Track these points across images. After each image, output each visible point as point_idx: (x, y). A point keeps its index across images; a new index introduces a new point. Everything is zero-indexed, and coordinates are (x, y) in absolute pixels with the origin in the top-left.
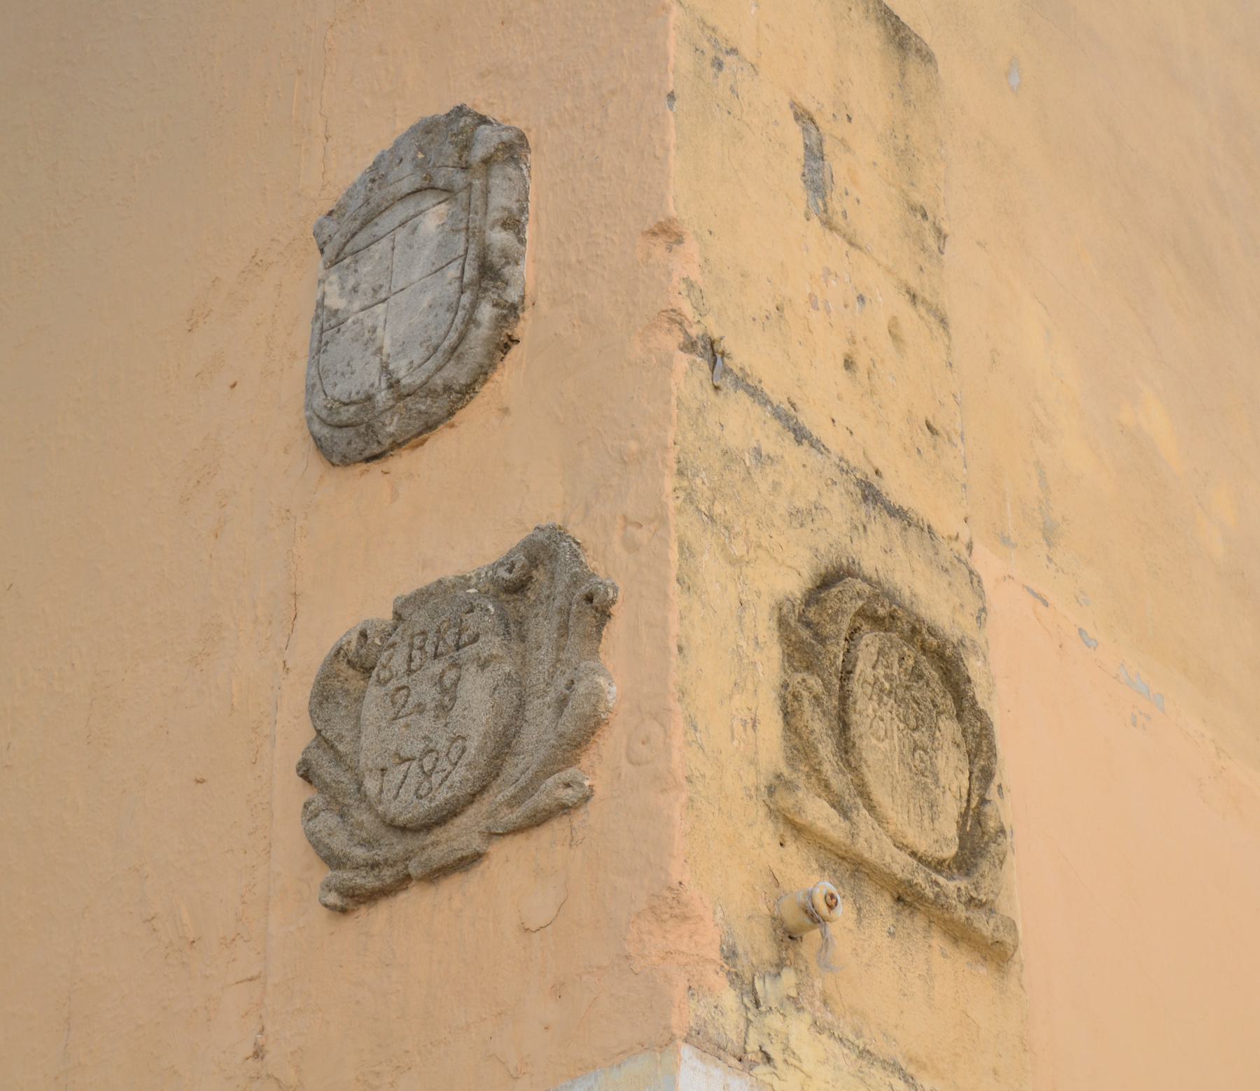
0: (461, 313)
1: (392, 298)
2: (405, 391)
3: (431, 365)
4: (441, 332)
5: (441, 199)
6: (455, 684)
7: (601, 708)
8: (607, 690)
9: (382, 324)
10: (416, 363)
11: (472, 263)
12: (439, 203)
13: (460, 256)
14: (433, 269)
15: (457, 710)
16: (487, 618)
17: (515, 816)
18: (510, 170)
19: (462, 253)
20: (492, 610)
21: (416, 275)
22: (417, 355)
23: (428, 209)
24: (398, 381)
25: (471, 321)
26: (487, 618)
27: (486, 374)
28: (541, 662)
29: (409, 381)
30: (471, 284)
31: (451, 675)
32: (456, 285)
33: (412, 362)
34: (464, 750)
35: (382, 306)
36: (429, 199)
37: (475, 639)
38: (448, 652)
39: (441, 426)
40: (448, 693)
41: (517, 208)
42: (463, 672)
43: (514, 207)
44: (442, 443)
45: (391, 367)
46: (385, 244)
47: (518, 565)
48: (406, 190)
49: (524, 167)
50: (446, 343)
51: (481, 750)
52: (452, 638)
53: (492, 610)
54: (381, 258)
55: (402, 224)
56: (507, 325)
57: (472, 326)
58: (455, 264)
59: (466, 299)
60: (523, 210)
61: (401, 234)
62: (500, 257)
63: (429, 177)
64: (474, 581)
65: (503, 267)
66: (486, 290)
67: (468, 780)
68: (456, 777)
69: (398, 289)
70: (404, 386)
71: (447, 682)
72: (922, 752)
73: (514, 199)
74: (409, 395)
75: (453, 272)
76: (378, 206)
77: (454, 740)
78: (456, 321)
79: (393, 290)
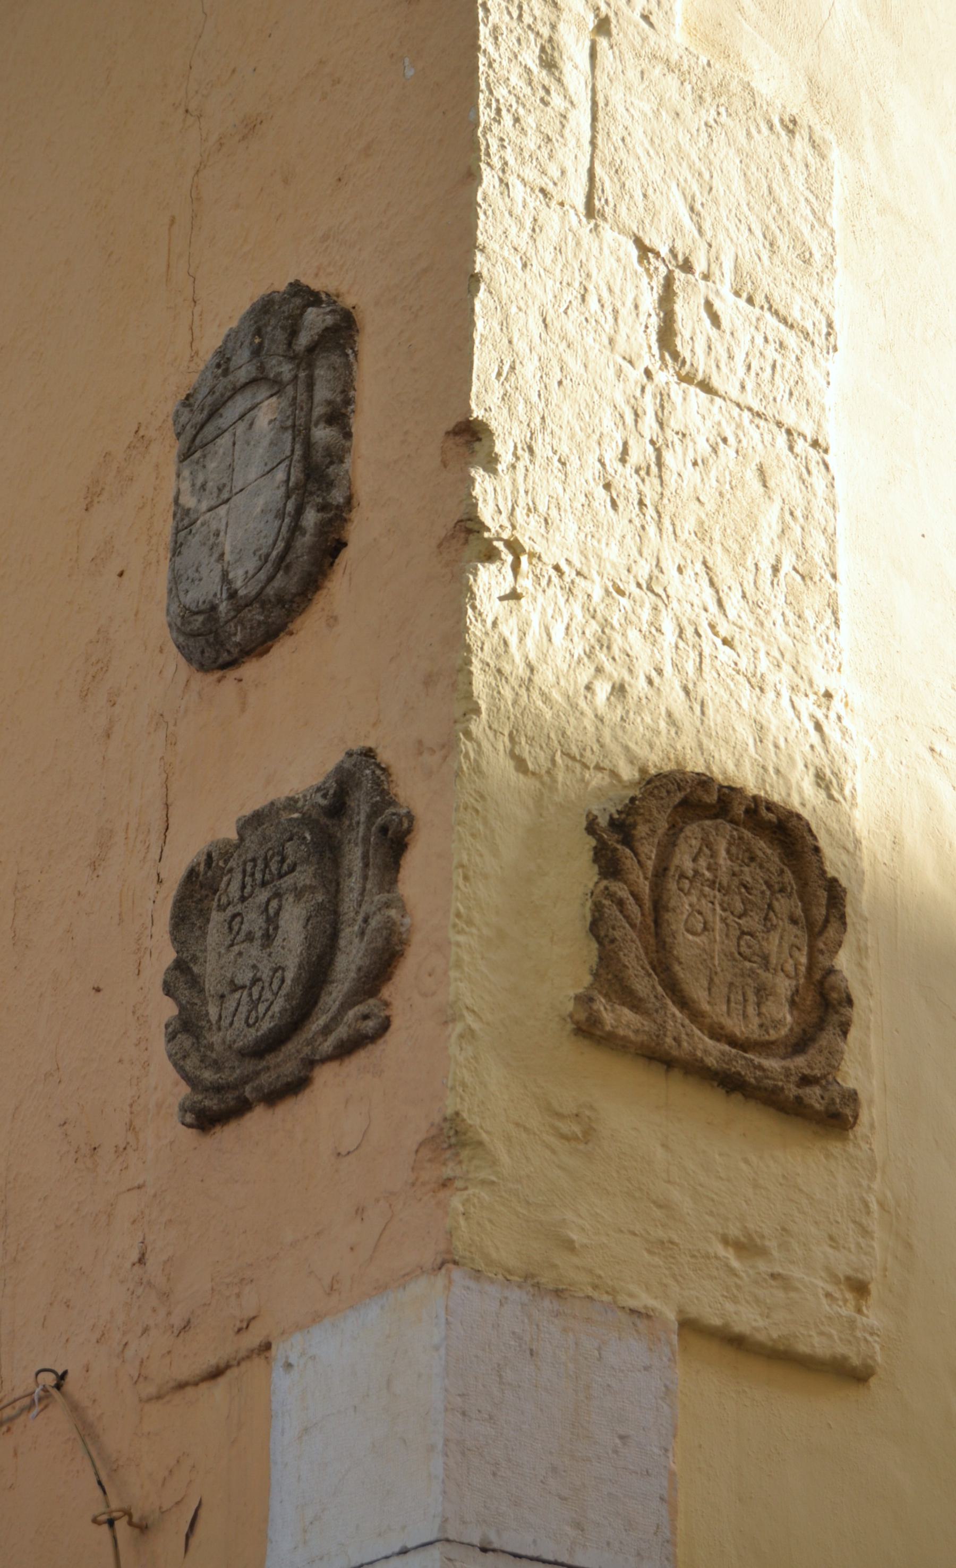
0: (287, 520)
1: (234, 498)
2: (242, 602)
3: (262, 576)
4: (270, 541)
5: (274, 391)
6: (277, 913)
7: (395, 939)
8: (399, 923)
9: (223, 528)
10: (251, 573)
11: (298, 465)
12: (272, 396)
13: (287, 457)
14: (267, 469)
15: (278, 941)
16: (303, 847)
17: (328, 1045)
18: (336, 359)
19: (288, 453)
20: (308, 837)
21: (253, 473)
22: (251, 564)
23: (262, 402)
24: (236, 592)
25: (296, 528)
26: (303, 847)
27: (316, 581)
28: (351, 890)
29: (245, 592)
30: (297, 487)
31: (274, 904)
32: (283, 489)
33: (247, 572)
34: (283, 981)
35: (224, 508)
36: (263, 392)
37: (292, 869)
38: (272, 881)
39: (282, 634)
40: (272, 921)
41: (342, 400)
42: (284, 902)
43: (338, 399)
44: (282, 651)
45: (231, 576)
46: (225, 440)
47: (331, 792)
48: (243, 380)
49: (350, 352)
50: (274, 553)
51: (296, 980)
52: (276, 866)
53: (308, 837)
54: (224, 454)
55: (241, 417)
56: (332, 529)
57: (297, 533)
58: (283, 466)
59: (290, 507)
60: (348, 402)
61: (241, 427)
62: (324, 457)
63: (261, 368)
64: (300, 804)
65: (328, 467)
66: (311, 494)
67: (286, 1010)
68: (276, 1008)
69: (237, 490)
70: (241, 597)
71: (271, 911)
72: (748, 937)
73: (338, 390)
74: (247, 606)
75: (280, 475)
76: (222, 395)
77: (275, 971)
78: (283, 529)
79: (234, 491)
